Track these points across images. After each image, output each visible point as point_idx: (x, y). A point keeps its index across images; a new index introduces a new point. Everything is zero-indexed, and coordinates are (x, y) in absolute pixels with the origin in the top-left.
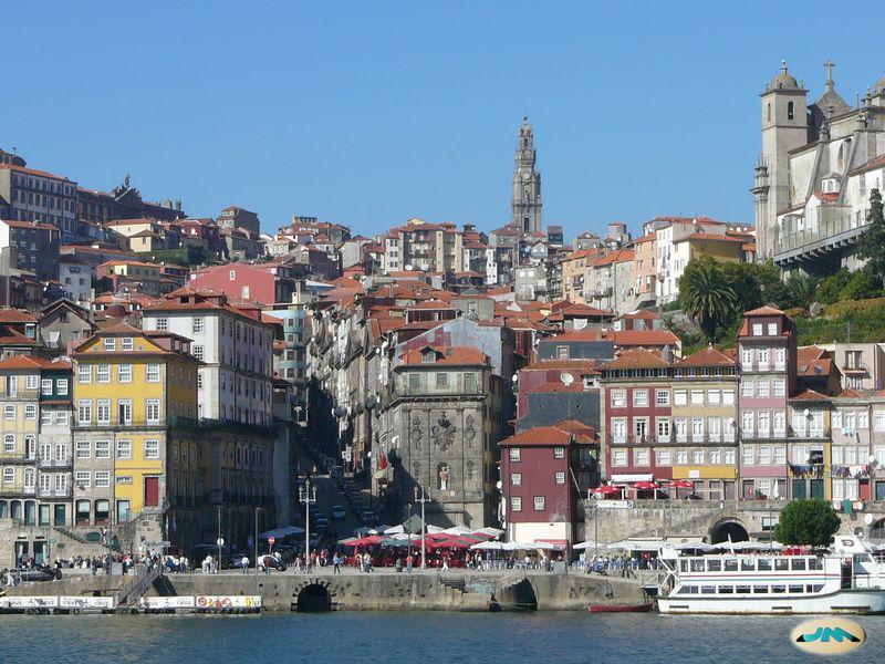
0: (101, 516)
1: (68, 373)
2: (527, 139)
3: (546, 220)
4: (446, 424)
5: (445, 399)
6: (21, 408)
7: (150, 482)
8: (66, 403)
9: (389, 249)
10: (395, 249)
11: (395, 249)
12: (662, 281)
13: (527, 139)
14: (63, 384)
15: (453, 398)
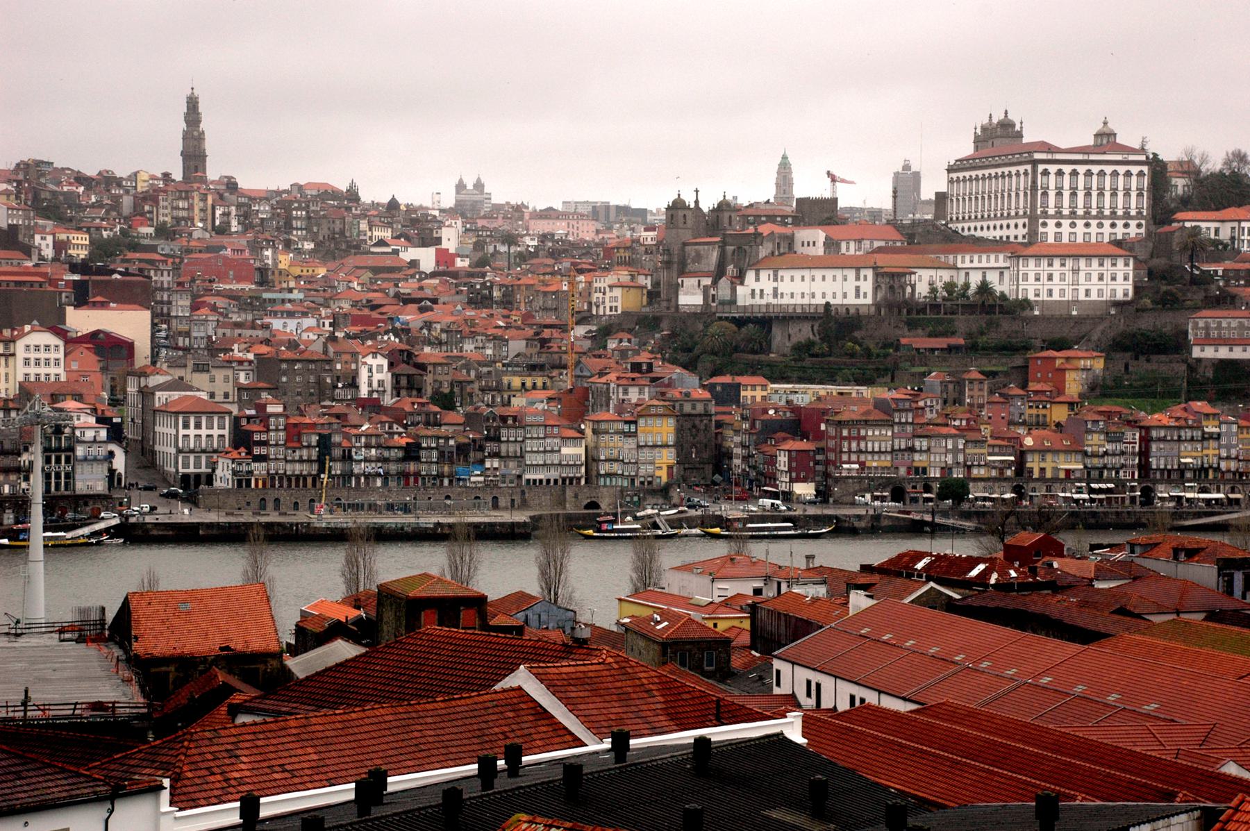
0: (650, 483)
1: (635, 422)
2: (193, 104)
3: (214, 172)
4: (694, 426)
5: (696, 415)
6: (616, 437)
7: (670, 468)
8: (635, 435)
9: (161, 203)
10: (165, 204)
11: (165, 204)
12: (598, 307)
13: (193, 104)
14: (633, 428)
15: (700, 415)
